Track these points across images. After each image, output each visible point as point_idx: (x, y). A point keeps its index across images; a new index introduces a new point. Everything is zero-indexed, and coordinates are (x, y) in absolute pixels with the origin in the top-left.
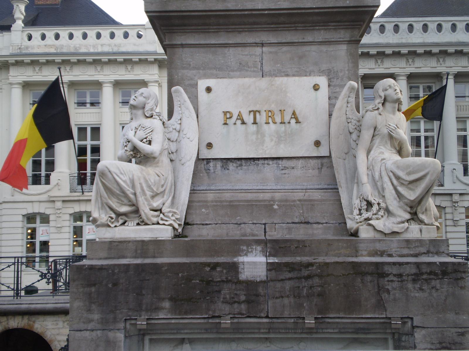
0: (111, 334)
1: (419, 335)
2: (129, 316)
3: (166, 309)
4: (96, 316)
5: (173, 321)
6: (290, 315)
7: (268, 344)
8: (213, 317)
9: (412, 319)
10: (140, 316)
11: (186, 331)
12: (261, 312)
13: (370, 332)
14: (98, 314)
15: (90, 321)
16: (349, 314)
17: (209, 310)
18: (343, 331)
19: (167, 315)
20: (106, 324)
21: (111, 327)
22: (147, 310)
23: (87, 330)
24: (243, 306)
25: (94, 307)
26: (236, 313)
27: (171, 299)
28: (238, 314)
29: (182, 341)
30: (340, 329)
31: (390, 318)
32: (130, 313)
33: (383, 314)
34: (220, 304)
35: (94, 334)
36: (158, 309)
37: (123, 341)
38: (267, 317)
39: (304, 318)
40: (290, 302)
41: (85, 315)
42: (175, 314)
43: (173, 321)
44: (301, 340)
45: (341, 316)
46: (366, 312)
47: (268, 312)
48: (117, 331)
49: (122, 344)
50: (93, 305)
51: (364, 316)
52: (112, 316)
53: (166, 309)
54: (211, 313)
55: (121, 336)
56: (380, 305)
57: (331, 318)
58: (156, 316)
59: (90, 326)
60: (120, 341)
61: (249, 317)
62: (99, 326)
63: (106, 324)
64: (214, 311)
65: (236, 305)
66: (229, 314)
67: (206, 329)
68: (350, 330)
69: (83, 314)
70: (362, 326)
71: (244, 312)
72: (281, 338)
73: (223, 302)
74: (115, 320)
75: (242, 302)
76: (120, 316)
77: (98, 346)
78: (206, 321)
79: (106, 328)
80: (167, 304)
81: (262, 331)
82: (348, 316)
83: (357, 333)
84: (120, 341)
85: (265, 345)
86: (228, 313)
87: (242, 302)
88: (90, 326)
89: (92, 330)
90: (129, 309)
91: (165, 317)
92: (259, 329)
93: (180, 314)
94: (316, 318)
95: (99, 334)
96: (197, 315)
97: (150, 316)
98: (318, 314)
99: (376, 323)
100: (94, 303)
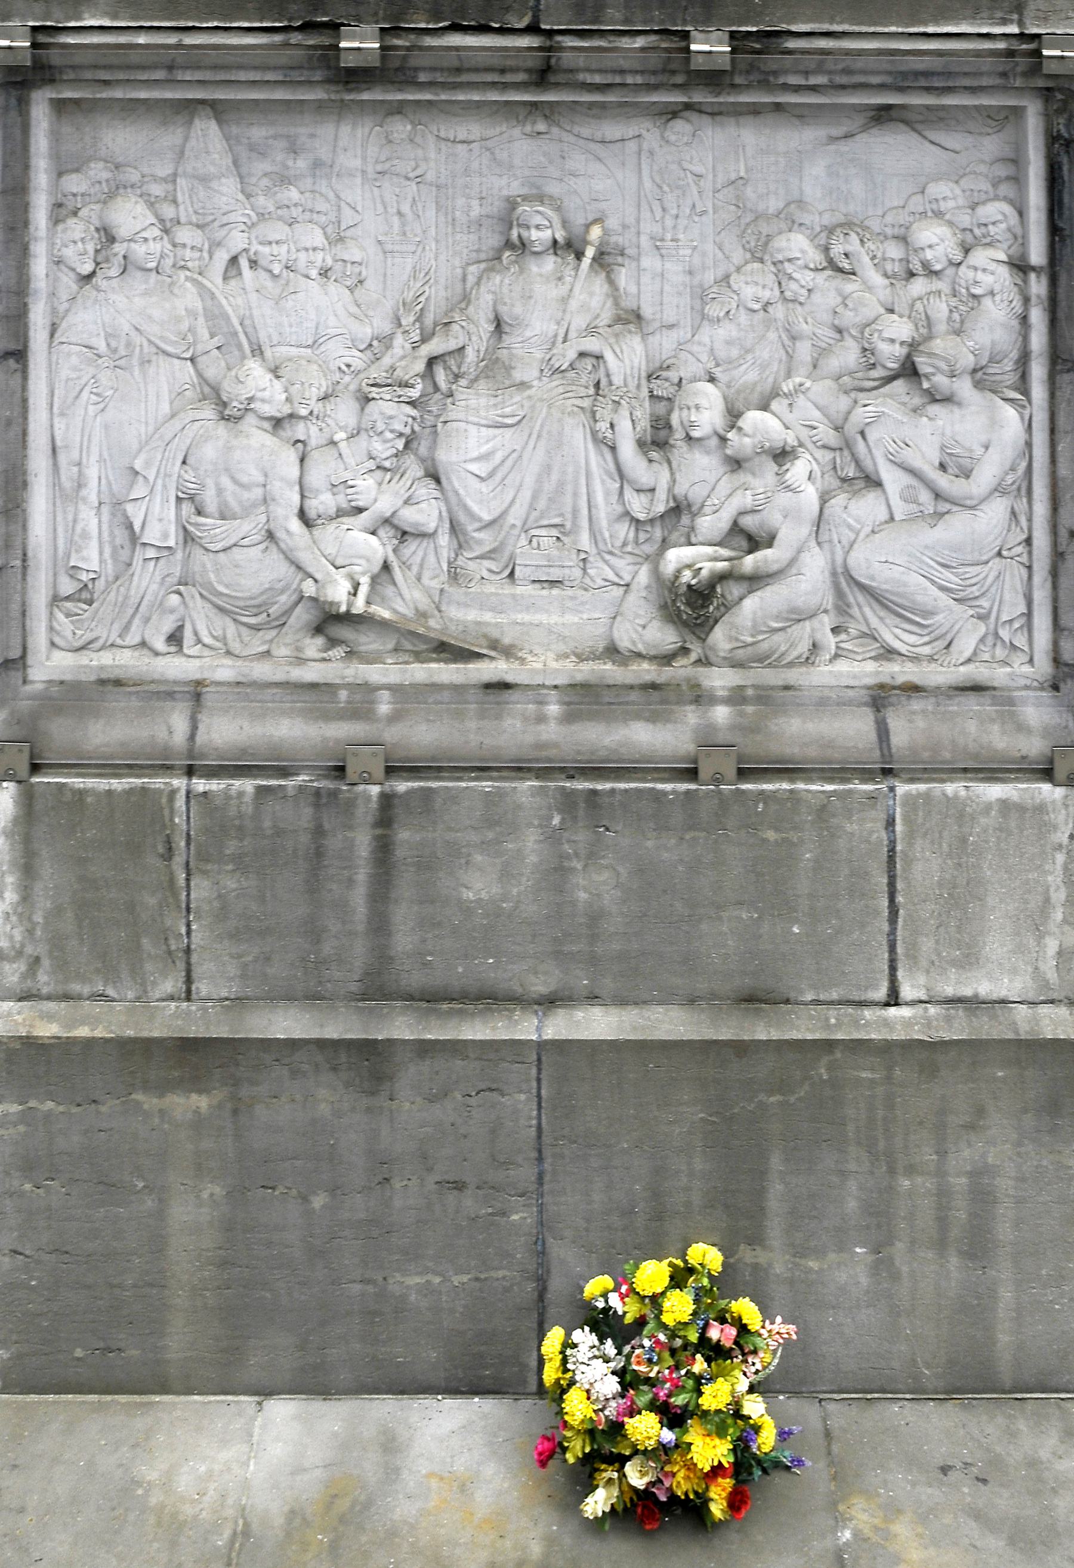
7: (541, 127)
13: (950, 84)
29: (188, 108)
33: (1011, 21)
44: (672, 113)
72: (591, 105)
83: (901, 90)
85: (528, 129)
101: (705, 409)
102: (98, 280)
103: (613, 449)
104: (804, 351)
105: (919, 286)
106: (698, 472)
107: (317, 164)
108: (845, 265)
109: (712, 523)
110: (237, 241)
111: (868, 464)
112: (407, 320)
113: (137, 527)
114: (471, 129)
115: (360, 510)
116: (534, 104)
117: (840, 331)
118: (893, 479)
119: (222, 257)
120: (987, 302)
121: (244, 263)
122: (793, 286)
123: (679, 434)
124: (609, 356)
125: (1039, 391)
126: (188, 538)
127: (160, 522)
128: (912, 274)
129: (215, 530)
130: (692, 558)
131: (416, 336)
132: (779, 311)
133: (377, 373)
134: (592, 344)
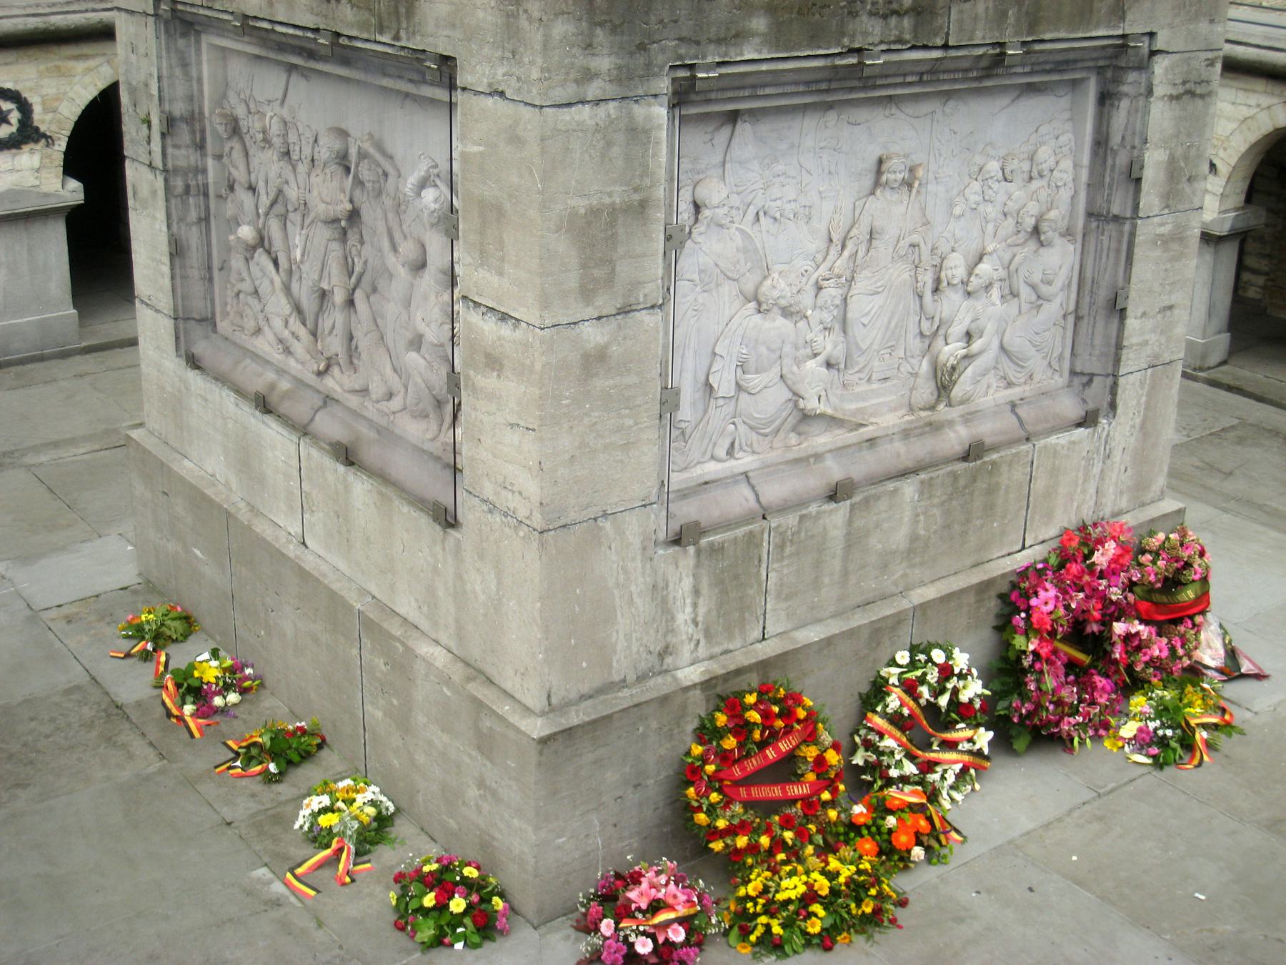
0: (639, 111)
1: (1160, 66)
2: (680, 57)
3: (758, 35)
4: (604, 63)
5: (764, 67)
6: (984, 38)
7: (894, 110)
8: (852, 51)
9: (1152, 35)
10: (704, 57)
11: (768, 91)
12: (936, 35)
14: (610, 55)
15: (588, 75)
16: (1073, 31)
17: (843, 35)
18: (1036, 68)
19: (760, 52)
20: (628, 83)
21: (640, 92)
22: (719, 41)
23: (583, 102)
24: (907, 22)
25: (600, 35)
26: (892, 38)
27: (771, 10)
28: (895, 42)
29: (733, 117)
30: (1033, 64)
31: (1124, 36)
32: (682, 51)
34: (864, 18)
35: (601, 111)
36: (740, 36)
37: (665, 127)
38: (946, 47)
39: (1002, 45)
40: (987, 8)
41: (581, 60)
42: (777, 51)
43: (764, 67)
45: (1063, 35)
46: (1097, 27)
47: (947, 34)
48: (652, 100)
49: (663, 134)
50: (598, 31)
51: (1094, 34)
52: (641, 60)
53: (758, 35)
54: (846, 41)
55: (660, 112)
56: (1119, 11)
57: (1051, 41)
58: (737, 55)
59: (593, 90)
60: (659, 127)
61: (914, 48)
62: (611, 90)
63: (628, 83)
64: (853, 38)
65: (893, 21)
66: (882, 42)
67: (807, 83)
68: (1048, 67)
69: (574, 56)
70: (1071, 56)
71: (907, 37)
73: (871, 14)
74: (649, 72)
75: (906, 12)
76: (660, 59)
77: (609, 144)
78: (828, 62)
79: (630, 94)
80: (759, 23)
81: (909, 79)
82: (1072, 36)
84: (659, 127)
85: (887, 112)
86: (877, 40)
87: (906, 12)
88: (593, 90)
89: (598, 102)
90: (681, 39)
91: (756, 57)
92: (905, 75)
93: (787, 49)
94: (1024, 43)
95: (612, 111)
96: (820, 47)
97: (726, 55)
98: (1029, 34)
99: (1095, 48)
100: (601, 24)
101: (956, 267)
102: (693, 235)
103: (921, 297)
104: (990, 228)
105: (1035, 184)
106: (952, 302)
107: (792, 146)
108: (1009, 177)
109: (957, 330)
110: (759, 202)
111: (1015, 286)
112: (835, 237)
113: (715, 386)
114: (862, 114)
115: (816, 355)
116: (890, 97)
117: (1005, 215)
118: (1025, 292)
119: (752, 211)
120: (1062, 189)
121: (761, 214)
122: (990, 192)
123: (945, 284)
124: (922, 245)
125: (1079, 238)
126: (739, 387)
127: (724, 382)
128: (1031, 178)
129: (754, 381)
130: (951, 351)
131: (839, 247)
132: (981, 208)
133: (823, 271)
134: (915, 238)
